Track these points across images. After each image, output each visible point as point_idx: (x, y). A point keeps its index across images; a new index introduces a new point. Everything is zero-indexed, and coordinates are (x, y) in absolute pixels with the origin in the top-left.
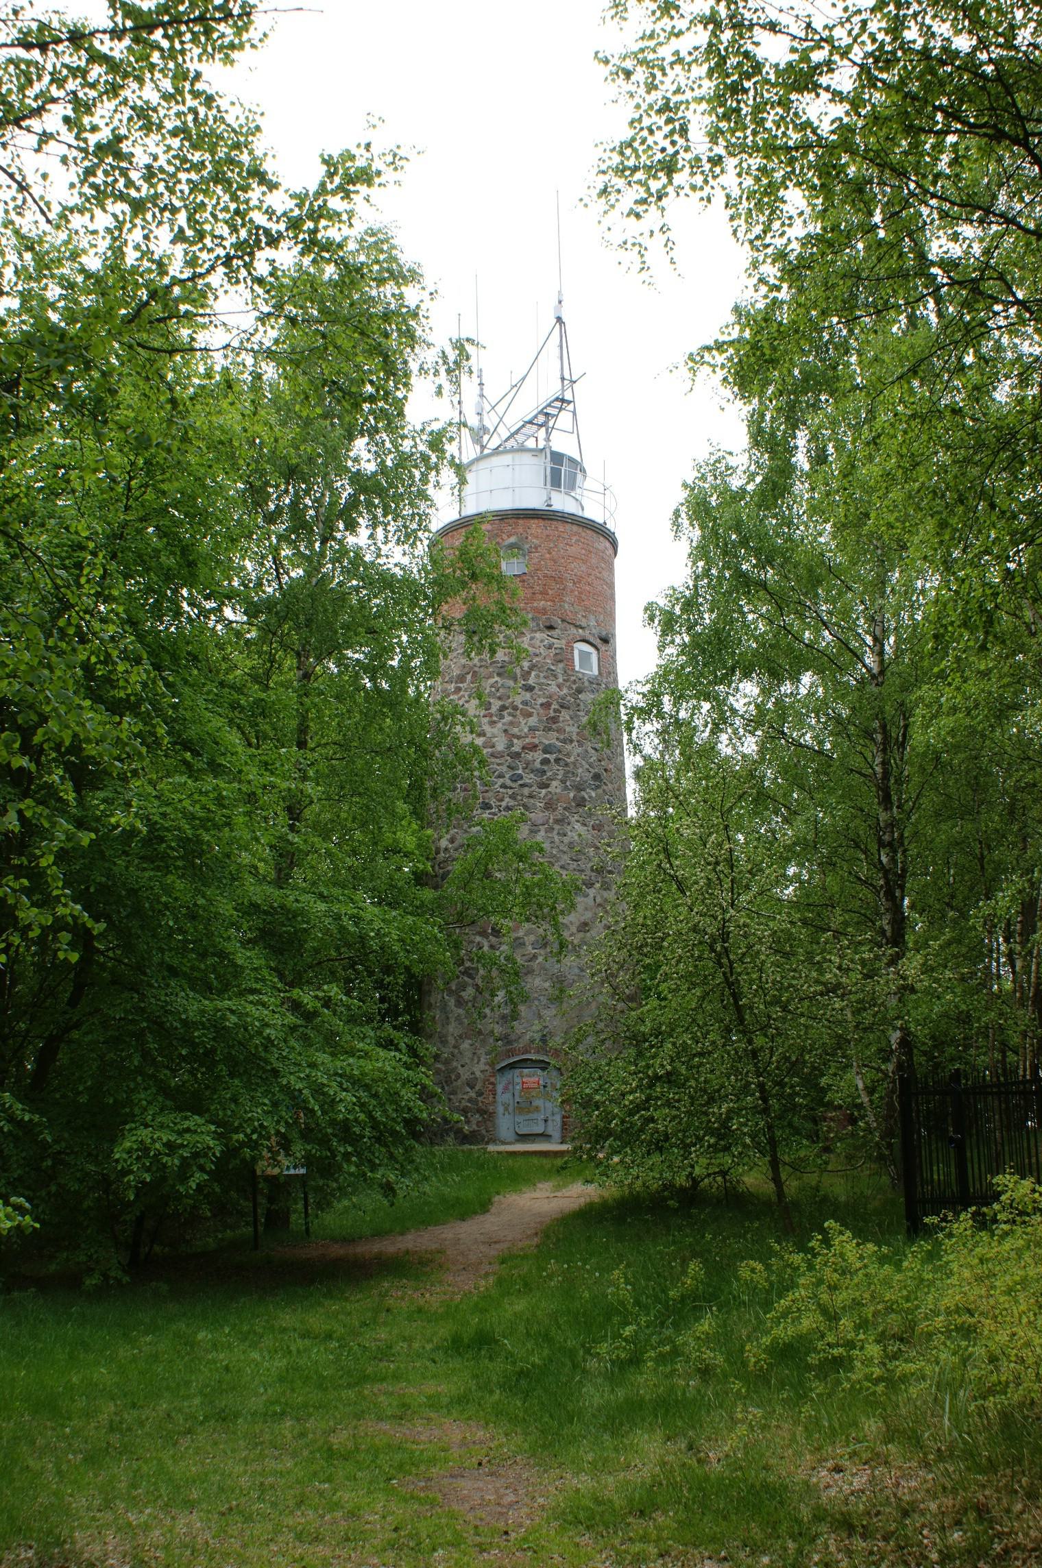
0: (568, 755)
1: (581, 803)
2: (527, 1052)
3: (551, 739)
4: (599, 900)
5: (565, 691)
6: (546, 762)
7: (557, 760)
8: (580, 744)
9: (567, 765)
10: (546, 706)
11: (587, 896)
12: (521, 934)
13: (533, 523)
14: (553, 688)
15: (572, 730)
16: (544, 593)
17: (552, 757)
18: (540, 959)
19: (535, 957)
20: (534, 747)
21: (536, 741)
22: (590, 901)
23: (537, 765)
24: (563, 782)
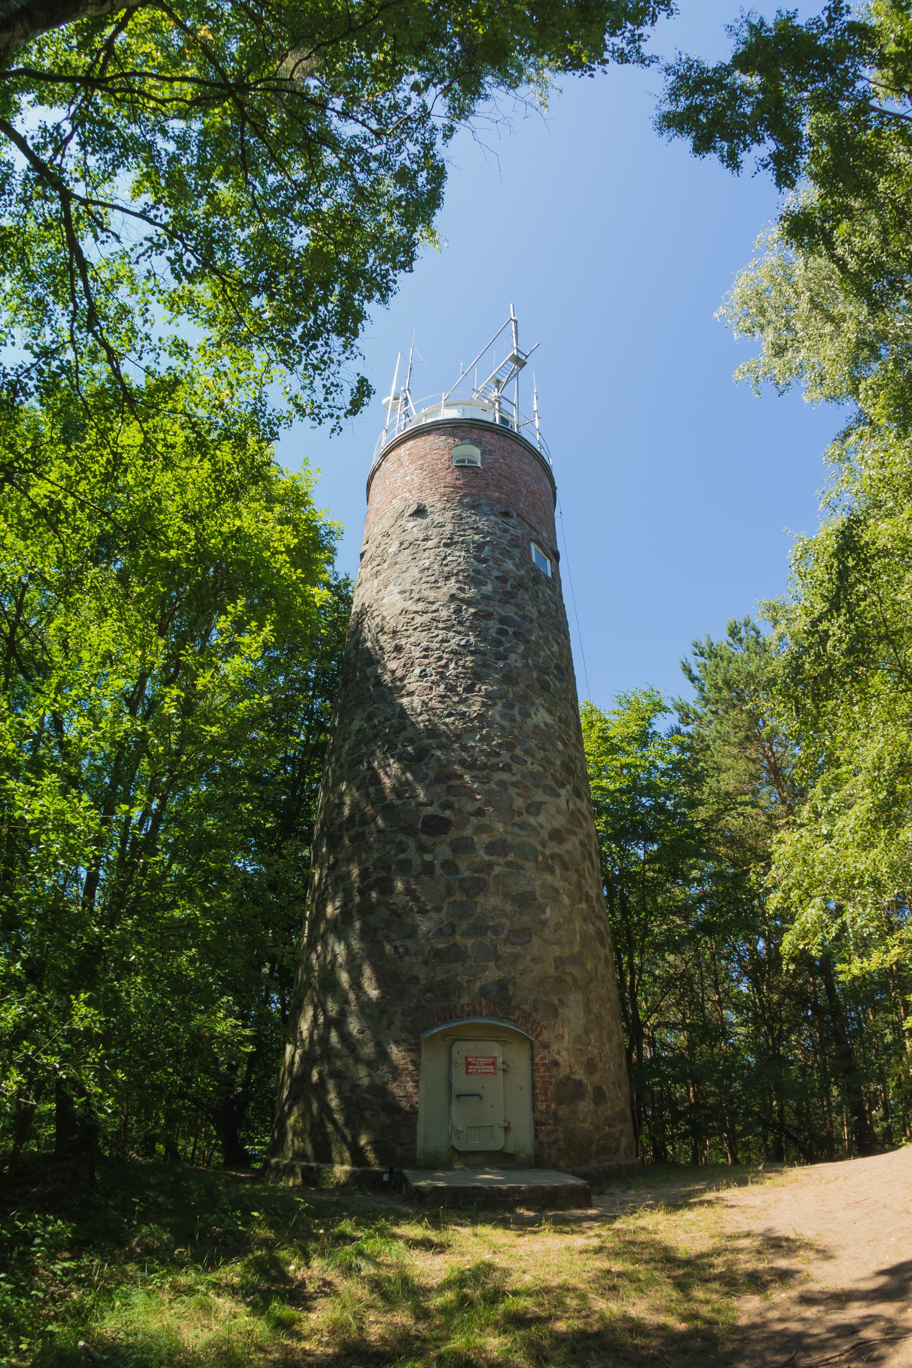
0: (530, 632)
1: (545, 687)
2: (474, 1013)
3: (510, 611)
4: (571, 806)
5: (522, 572)
6: (501, 632)
7: (515, 634)
8: (541, 628)
9: (527, 642)
10: (503, 579)
11: (559, 796)
12: (468, 831)
13: (488, 436)
14: (509, 565)
15: (533, 612)
16: (499, 487)
17: (511, 631)
18: (497, 870)
19: (490, 866)
20: (489, 616)
21: (491, 609)
22: (562, 802)
23: (493, 632)
24: (524, 656)
